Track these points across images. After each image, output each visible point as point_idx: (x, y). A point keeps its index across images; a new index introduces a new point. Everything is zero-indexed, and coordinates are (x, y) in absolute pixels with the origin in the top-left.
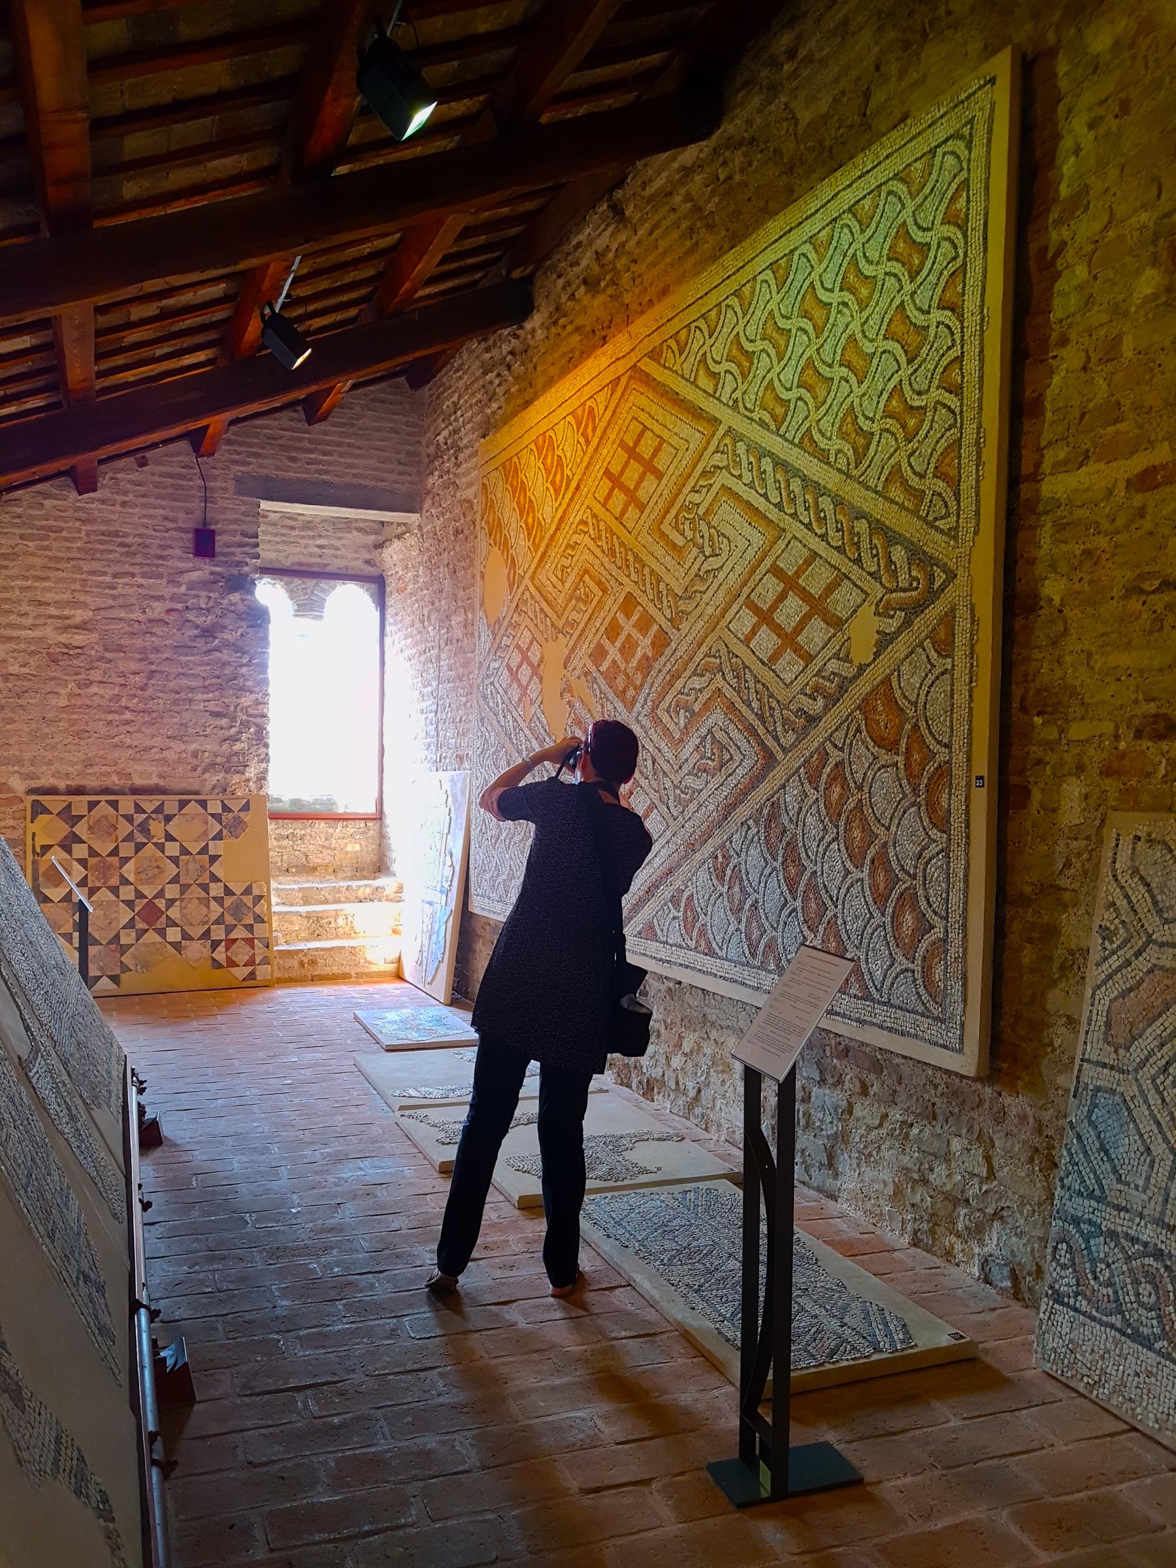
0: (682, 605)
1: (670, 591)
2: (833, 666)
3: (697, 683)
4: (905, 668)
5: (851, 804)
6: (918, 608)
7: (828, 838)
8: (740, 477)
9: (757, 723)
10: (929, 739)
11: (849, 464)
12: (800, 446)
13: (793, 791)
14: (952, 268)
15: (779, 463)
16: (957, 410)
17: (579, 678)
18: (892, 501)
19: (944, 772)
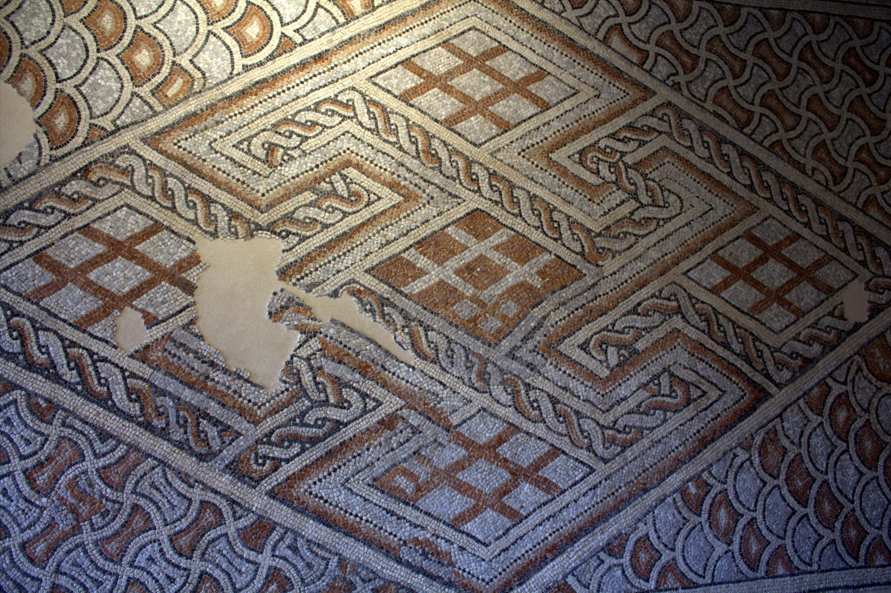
0: (601, 242)
1: (572, 223)
2: (828, 321)
3: (639, 322)
5: (859, 423)
7: (837, 452)
8: (691, 148)
9: (739, 363)
11: (827, 181)
12: (771, 148)
13: (793, 418)
15: (743, 154)
17: (335, 294)
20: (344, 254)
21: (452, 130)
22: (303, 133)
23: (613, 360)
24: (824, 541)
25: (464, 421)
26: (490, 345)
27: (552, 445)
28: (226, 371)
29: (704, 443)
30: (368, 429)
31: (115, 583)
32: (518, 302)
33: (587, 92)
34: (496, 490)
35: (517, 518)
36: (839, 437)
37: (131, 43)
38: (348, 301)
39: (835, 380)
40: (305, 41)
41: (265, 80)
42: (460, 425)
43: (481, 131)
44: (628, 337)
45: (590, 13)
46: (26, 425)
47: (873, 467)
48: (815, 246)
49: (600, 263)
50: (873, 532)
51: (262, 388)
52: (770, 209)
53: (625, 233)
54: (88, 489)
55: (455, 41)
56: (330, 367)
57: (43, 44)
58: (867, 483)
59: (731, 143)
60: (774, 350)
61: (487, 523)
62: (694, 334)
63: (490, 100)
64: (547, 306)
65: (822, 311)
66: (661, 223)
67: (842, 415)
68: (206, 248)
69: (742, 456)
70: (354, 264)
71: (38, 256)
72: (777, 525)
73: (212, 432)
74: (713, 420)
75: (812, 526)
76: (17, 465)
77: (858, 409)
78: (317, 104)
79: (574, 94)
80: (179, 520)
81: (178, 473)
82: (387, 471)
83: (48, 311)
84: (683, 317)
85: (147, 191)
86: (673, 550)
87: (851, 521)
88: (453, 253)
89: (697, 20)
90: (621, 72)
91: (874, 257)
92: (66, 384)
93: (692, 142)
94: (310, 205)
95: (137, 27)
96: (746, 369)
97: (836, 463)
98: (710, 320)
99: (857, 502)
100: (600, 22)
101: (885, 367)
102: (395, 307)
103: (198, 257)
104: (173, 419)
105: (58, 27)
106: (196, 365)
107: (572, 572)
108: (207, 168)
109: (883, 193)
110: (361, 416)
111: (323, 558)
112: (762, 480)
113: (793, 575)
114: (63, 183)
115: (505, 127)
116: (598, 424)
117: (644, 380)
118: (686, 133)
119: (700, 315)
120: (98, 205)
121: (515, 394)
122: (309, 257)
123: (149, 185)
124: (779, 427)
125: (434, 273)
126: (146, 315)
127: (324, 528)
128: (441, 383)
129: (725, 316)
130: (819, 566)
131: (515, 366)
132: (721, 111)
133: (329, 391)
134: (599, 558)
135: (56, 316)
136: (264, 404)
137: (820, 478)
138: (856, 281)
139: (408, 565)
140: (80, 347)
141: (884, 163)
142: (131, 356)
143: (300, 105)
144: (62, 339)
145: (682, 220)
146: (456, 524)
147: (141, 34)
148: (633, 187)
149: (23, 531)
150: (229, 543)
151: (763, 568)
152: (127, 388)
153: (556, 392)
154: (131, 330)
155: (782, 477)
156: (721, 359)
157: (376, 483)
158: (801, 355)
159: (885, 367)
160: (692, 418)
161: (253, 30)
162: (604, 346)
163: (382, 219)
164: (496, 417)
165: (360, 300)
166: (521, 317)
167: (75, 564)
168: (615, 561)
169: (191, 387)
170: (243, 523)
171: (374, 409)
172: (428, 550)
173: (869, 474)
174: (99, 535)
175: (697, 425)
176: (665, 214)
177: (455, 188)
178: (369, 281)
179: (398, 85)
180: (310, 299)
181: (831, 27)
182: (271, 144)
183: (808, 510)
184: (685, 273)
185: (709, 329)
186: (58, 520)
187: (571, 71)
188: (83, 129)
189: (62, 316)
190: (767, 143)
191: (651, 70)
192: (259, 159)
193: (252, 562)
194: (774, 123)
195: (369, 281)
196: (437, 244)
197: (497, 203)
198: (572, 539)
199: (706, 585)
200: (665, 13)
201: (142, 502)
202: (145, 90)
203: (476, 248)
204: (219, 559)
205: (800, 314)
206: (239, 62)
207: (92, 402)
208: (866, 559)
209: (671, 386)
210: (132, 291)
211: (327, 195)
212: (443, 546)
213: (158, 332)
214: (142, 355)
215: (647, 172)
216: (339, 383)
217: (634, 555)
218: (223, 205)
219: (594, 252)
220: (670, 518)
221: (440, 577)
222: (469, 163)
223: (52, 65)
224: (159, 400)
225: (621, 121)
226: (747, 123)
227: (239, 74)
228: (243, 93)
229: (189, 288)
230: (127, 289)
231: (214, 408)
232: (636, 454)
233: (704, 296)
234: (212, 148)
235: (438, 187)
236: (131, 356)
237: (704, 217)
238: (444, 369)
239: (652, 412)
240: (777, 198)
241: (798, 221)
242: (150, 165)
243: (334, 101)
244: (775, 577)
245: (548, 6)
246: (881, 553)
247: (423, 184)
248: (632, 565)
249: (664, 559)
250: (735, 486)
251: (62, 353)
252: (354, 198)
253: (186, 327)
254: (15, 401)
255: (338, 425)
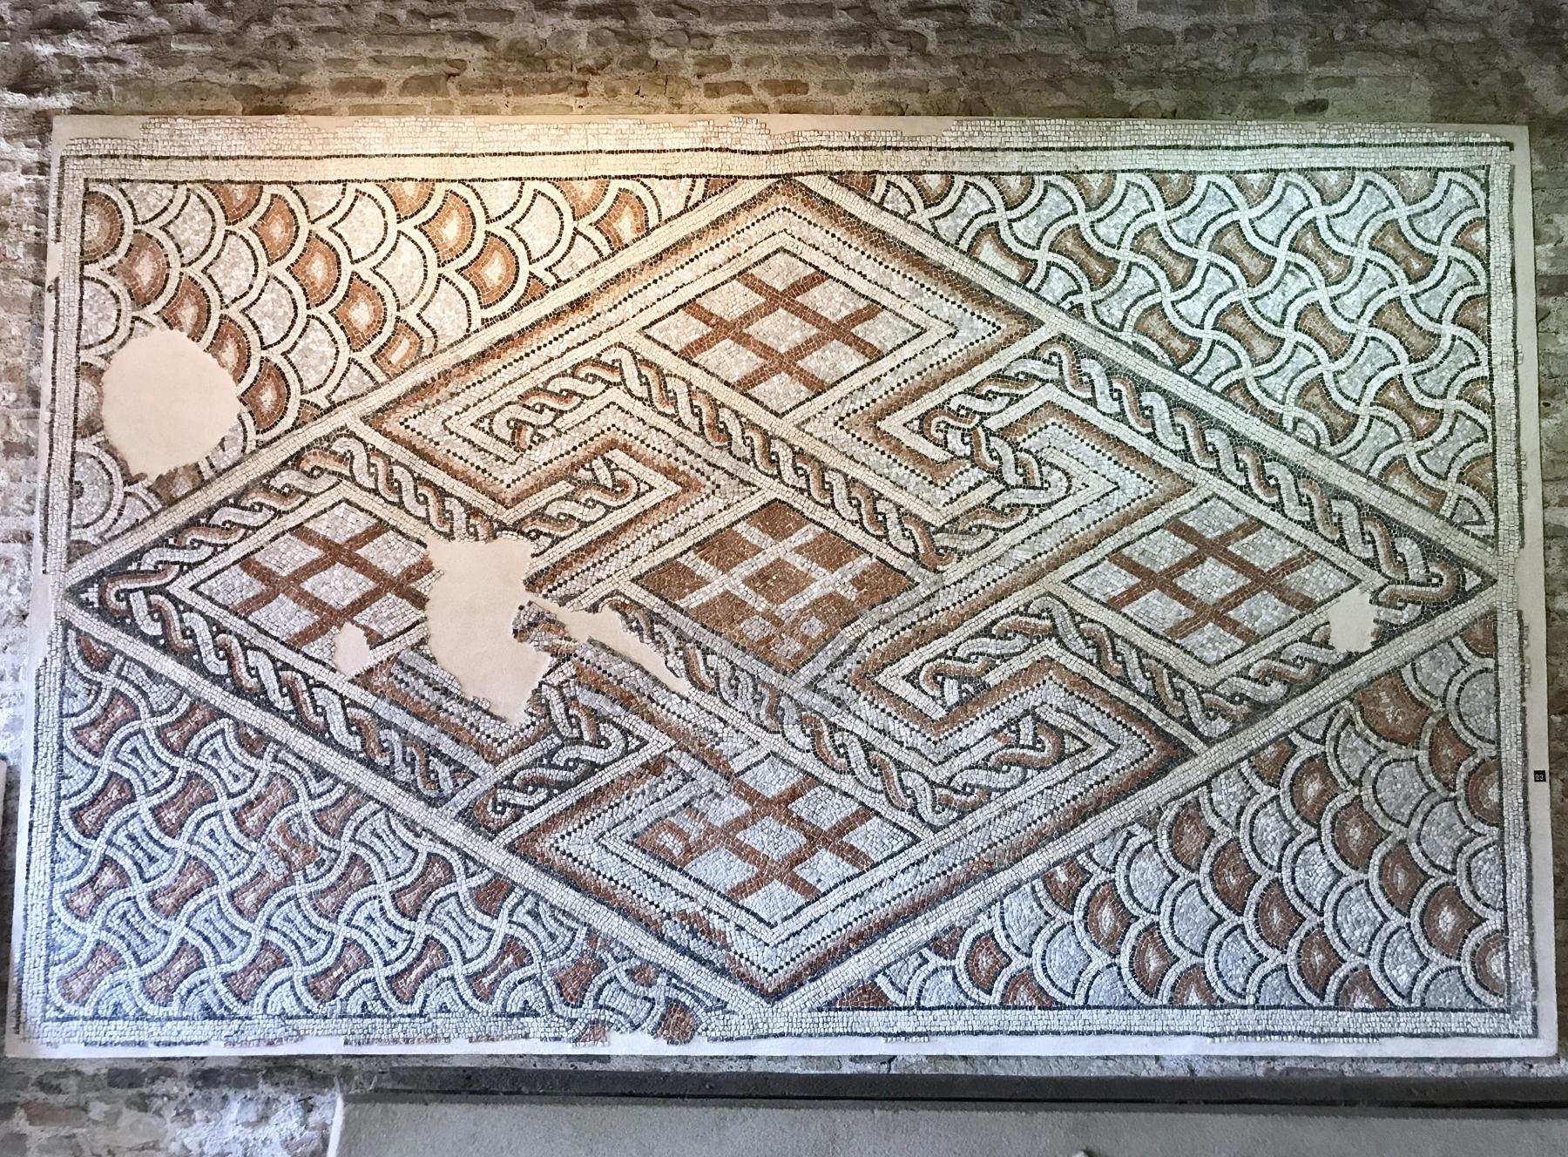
0: (942, 540)
1: (904, 515)
2: (1300, 649)
3: (992, 646)
4: (1424, 662)
5: (1341, 801)
6: (1440, 607)
7: (1300, 840)
8: (1092, 402)
10: (1465, 735)
11: (1318, 438)
12: (1225, 394)
14: (1469, 291)
15: (1175, 404)
16: (1489, 428)
17: (594, 608)
18: (1395, 492)
19: (1492, 768)
20: (607, 559)
21: (746, 395)
22: (557, 406)
23: (952, 697)
24: (1268, 966)
25: (749, 768)
26: (785, 674)
27: (861, 803)
28: (461, 700)
29: (1083, 815)
30: (628, 774)
31: (330, 943)
32: (824, 618)
33: (938, 330)
34: (785, 858)
35: (812, 894)
36: (1304, 819)
37: (346, 295)
38: (609, 616)
39: (1304, 736)
40: (560, 282)
41: (509, 338)
42: (743, 772)
43: (787, 395)
44: (975, 667)
45: (950, 211)
46: (234, 759)
47: (1361, 864)
48: (1288, 538)
49: (940, 568)
50: (1352, 961)
51: (503, 720)
52: (1216, 484)
53: (980, 527)
54: (302, 835)
55: (754, 271)
56: (585, 697)
57: (245, 302)
58: (1349, 888)
59: (1157, 389)
60: (1201, 690)
61: (774, 898)
62: (1074, 665)
63: (800, 351)
64: (862, 624)
65: (1288, 635)
66: (1036, 510)
67: (1312, 788)
68: (439, 551)
69: (1142, 835)
70: (619, 572)
71: (245, 562)
72: (1192, 936)
73: (444, 772)
74: (1097, 783)
75: (1248, 942)
76: (224, 804)
77: (1341, 780)
78: (575, 367)
79: (919, 335)
80: (402, 874)
81: (403, 820)
82: (651, 825)
83: (257, 627)
84: (1060, 641)
85: (370, 484)
86: (1029, 955)
87: (1316, 939)
88: (743, 557)
89: (1120, 204)
90: (992, 295)
91: (1393, 552)
92: (278, 713)
93: (1093, 392)
94: (565, 498)
95: (354, 273)
96: (1155, 715)
97: (1296, 856)
98: (1102, 646)
99: (1328, 915)
100: (966, 221)
101: (1396, 719)
102: (667, 624)
103: (430, 563)
104: (398, 756)
105: (261, 279)
106: (427, 692)
107: (883, 971)
108: (439, 455)
109: (1419, 454)
110: (622, 757)
111: (569, 929)
112: (1170, 871)
113: (1214, 1008)
114: (272, 474)
115: (818, 388)
116: (926, 779)
117: (996, 725)
118: (1085, 379)
119: (1085, 639)
120: (313, 500)
121: (816, 736)
122: (564, 563)
123: (371, 475)
124: (1204, 800)
125: (717, 583)
126: (369, 632)
127: (572, 892)
128: (721, 719)
129: (1126, 641)
130: (1257, 1000)
131: (817, 701)
132: (1146, 342)
133: (583, 726)
134: (921, 955)
135: (266, 633)
136: (505, 741)
137: (1267, 876)
138: (1356, 589)
139: (672, 944)
140: (293, 669)
141: (1428, 405)
142: (352, 681)
143: (554, 368)
144: (274, 661)
145: (1069, 505)
146: (734, 896)
147: (358, 282)
148: (996, 463)
149: (231, 878)
150: (460, 904)
151: (1165, 991)
152: (347, 719)
153: (871, 736)
154: (350, 650)
155: (1205, 869)
156: (1114, 700)
157: (636, 841)
158: (1248, 698)
159: (1396, 719)
160: (1066, 780)
161: (494, 271)
162: (939, 678)
163: (654, 515)
164: (790, 764)
165: (625, 616)
166: (825, 640)
167: (287, 919)
168: (944, 963)
169: (420, 719)
170: (475, 882)
171: (637, 749)
172: (697, 926)
173: (1353, 876)
174: (313, 887)
175: (1072, 790)
176: (1042, 498)
177: (748, 473)
178: (636, 593)
179: (678, 337)
180: (564, 614)
181: (1356, 189)
182: (518, 421)
183: (1243, 919)
184: (1067, 581)
185: (1099, 658)
186: (268, 868)
187: (917, 301)
188: (293, 406)
189: (273, 633)
190: (1218, 387)
191: (1038, 289)
192: (503, 441)
193: (486, 929)
194: (1235, 354)
195: (636, 593)
196: (722, 546)
197: (802, 491)
198: (885, 927)
199: (1075, 1008)
200: (1069, 199)
201: (362, 852)
202: (364, 356)
203: (774, 551)
204: (449, 924)
205: (1251, 638)
206: (478, 314)
207: (307, 733)
208: (1336, 998)
209: (1035, 735)
210: (353, 604)
211: (586, 485)
212: (717, 923)
213: (382, 653)
214: (364, 680)
215: (1019, 439)
216: (596, 717)
217: (971, 957)
218: (459, 499)
219: (932, 554)
220: (1026, 912)
221: (711, 962)
222: (768, 439)
223: (256, 327)
224: (383, 734)
225: (988, 368)
226: (1190, 356)
227: (477, 331)
228: (483, 356)
229: (419, 601)
230: (347, 602)
231: (446, 745)
232: (980, 823)
233: (1094, 611)
234: (446, 428)
235: (726, 472)
236: (352, 681)
237: (1103, 501)
238: (726, 702)
239: (1005, 768)
240: (1229, 468)
241: (1261, 501)
242: (372, 451)
243: (597, 362)
244: (1182, 1007)
245: (889, 207)
246: (1365, 991)
247: (707, 469)
248: (967, 970)
249: (1013, 968)
250: (1127, 877)
251: (274, 677)
252: (619, 488)
253: (415, 648)
254: (222, 731)
255: (593, 768)
